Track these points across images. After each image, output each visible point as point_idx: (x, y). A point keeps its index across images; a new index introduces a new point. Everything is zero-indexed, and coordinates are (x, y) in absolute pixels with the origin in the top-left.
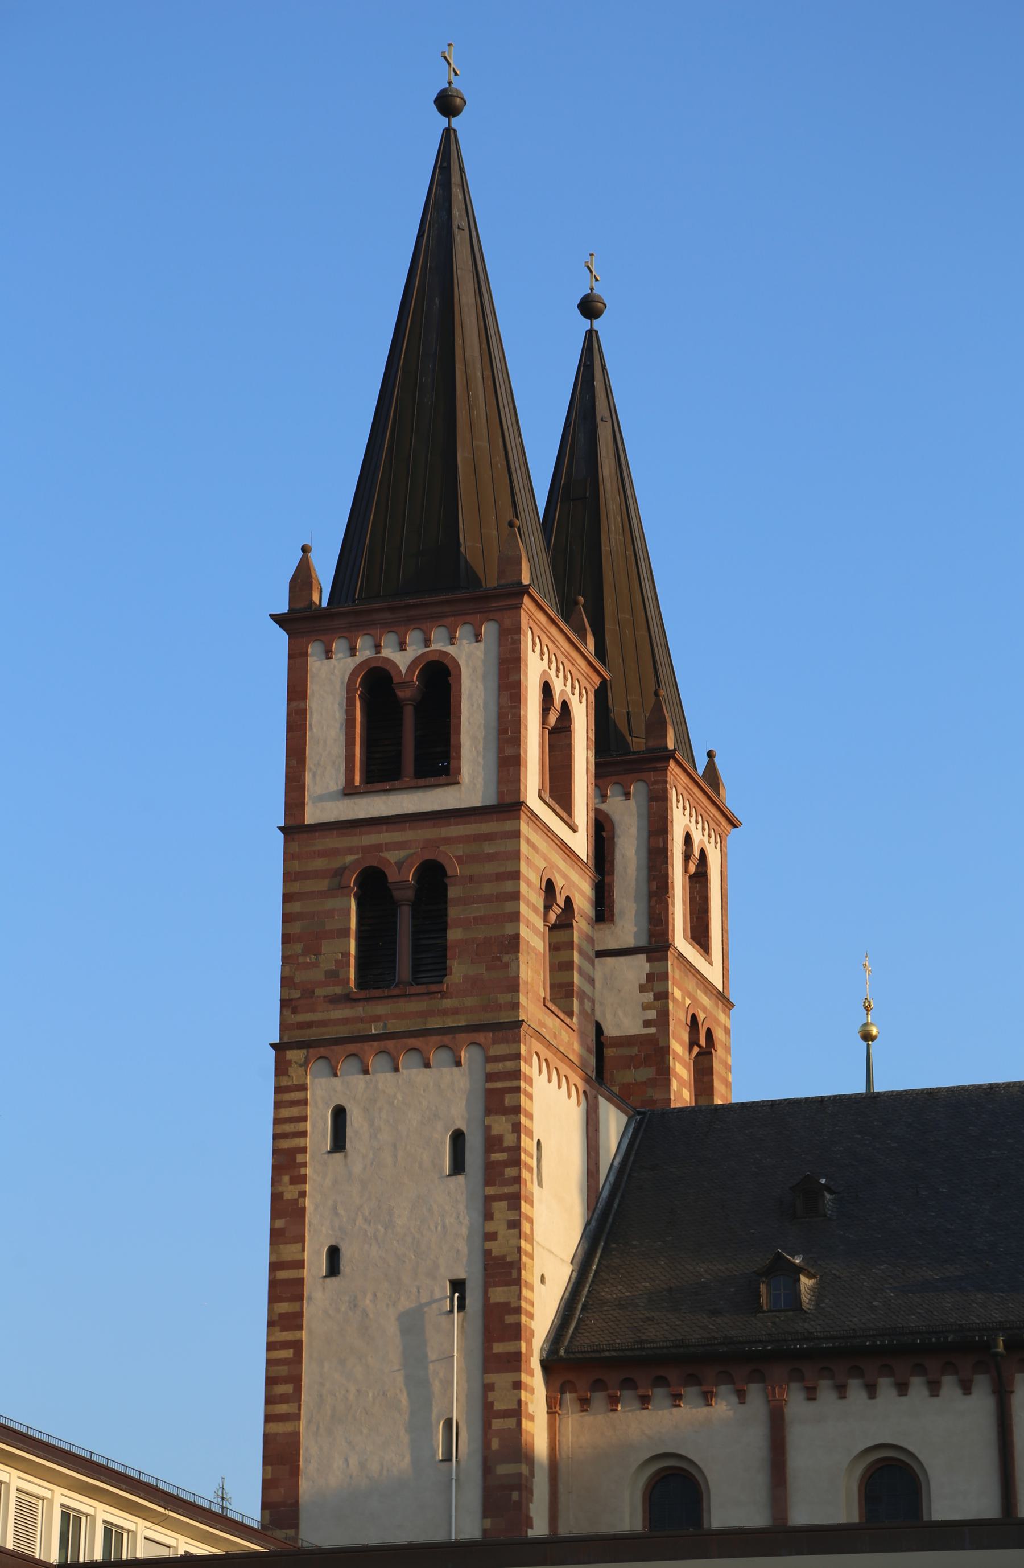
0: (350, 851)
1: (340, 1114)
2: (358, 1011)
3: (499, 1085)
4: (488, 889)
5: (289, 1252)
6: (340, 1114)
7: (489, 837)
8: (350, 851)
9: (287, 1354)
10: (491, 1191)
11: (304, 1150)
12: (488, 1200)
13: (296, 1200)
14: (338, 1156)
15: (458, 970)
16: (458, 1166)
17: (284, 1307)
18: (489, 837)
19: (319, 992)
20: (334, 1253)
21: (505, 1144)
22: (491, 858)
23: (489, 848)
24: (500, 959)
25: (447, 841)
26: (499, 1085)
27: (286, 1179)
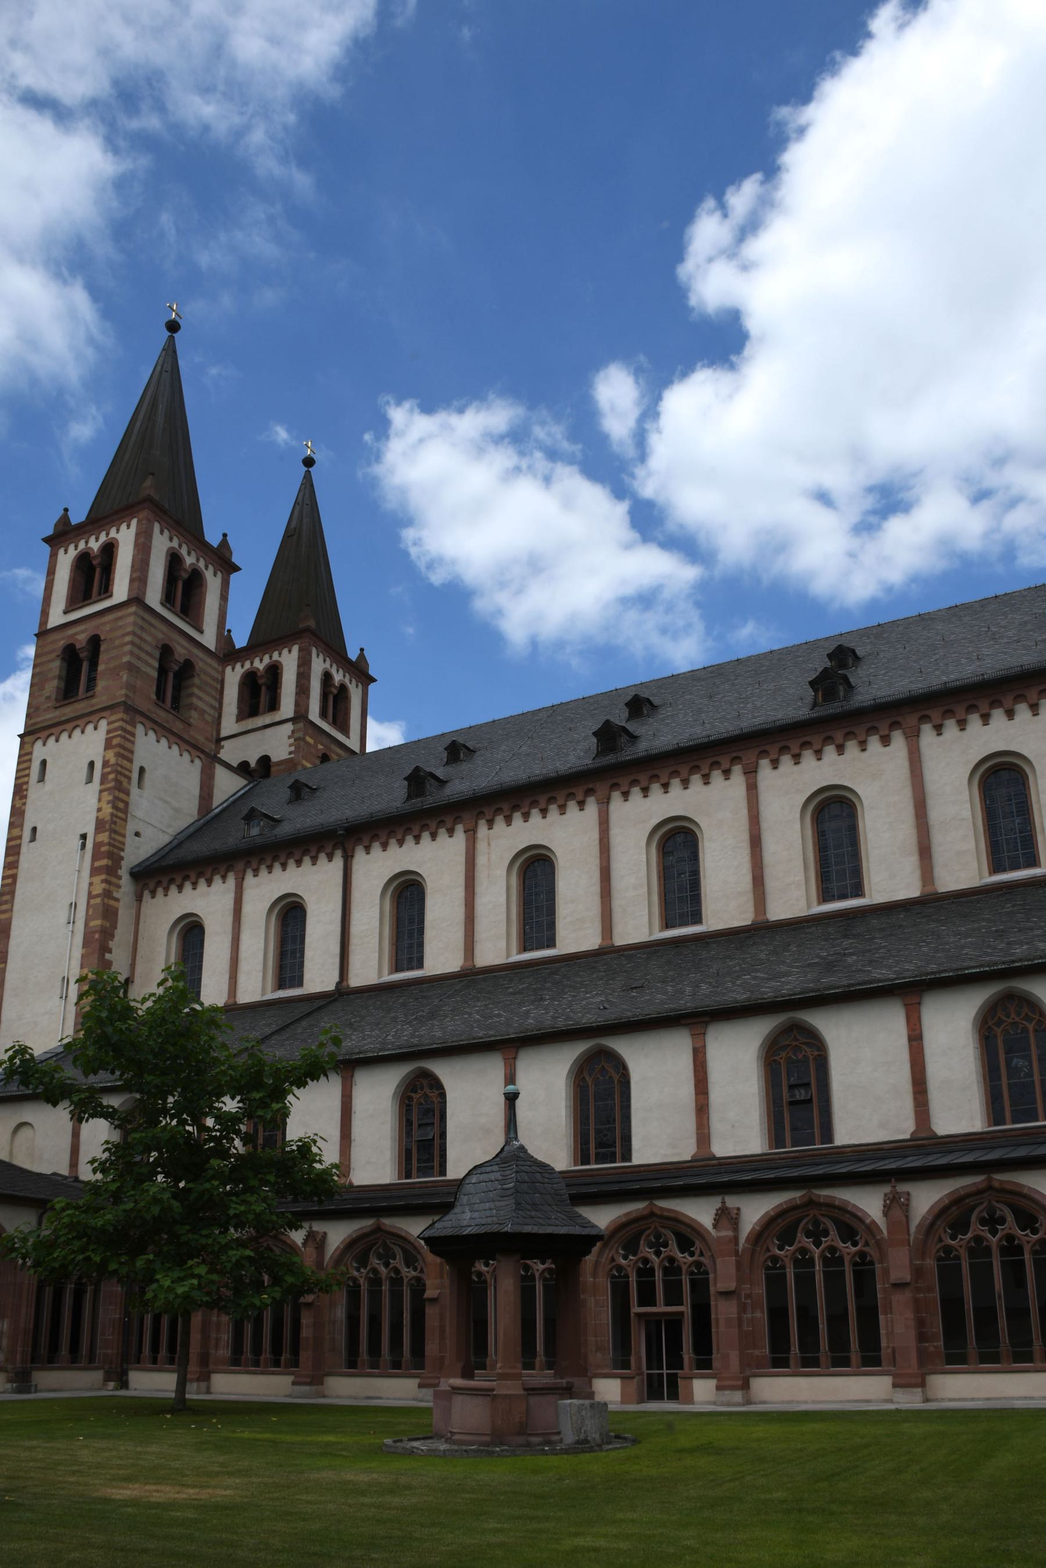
0: (62, 639)
1: (44, 763)
2: (57, 713)
3: (111, 735)
4: (117, 642)
5: (16, 832)
6: (44, 763)
7: (120, 618)
8: (62, 639)
9: (9, 881)
10: (104, 787)
11: (27, 783)
12: (101, 791)
13: (21, 807)
14: (41, 784)
15: (101, 684)
16: (90, 780)
17: (11, 859)
18: (120, 618)
19: (41, 708)
20: (34, 830)
21: (110, 763)
22: (121, 627)
23: (120, 623)
24: (118, 675)
25: (104, 624)
26: (111, 735)
27: (17, 798)
